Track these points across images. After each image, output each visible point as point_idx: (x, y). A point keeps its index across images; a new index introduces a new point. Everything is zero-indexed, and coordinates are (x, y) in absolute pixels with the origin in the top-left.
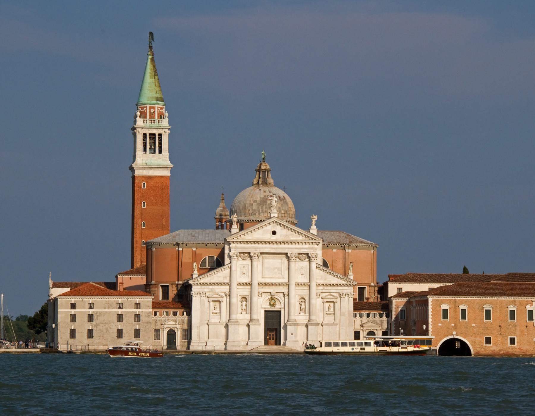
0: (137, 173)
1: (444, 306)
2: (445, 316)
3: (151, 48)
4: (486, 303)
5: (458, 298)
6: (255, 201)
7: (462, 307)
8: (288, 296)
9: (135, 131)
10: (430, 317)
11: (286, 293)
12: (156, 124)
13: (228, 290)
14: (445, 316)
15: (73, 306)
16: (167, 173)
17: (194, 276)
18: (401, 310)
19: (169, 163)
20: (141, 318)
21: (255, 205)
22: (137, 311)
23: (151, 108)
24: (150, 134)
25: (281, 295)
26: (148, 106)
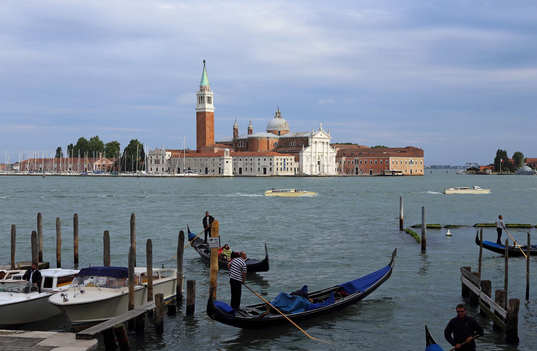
0: (207, 110)
1: (393, 160)
3: (204, 65)
4: (402, 159)
5: (396, 158)
6: (284, 123)
9: (205, 95)
12: (210, 93)
13: (310, 154)
14: (393, 164)
15: (277, 160)
16: (213, 111)
17: (304, 149)
19: (213, 107)
23: (208, 87)
25: (321, 156)
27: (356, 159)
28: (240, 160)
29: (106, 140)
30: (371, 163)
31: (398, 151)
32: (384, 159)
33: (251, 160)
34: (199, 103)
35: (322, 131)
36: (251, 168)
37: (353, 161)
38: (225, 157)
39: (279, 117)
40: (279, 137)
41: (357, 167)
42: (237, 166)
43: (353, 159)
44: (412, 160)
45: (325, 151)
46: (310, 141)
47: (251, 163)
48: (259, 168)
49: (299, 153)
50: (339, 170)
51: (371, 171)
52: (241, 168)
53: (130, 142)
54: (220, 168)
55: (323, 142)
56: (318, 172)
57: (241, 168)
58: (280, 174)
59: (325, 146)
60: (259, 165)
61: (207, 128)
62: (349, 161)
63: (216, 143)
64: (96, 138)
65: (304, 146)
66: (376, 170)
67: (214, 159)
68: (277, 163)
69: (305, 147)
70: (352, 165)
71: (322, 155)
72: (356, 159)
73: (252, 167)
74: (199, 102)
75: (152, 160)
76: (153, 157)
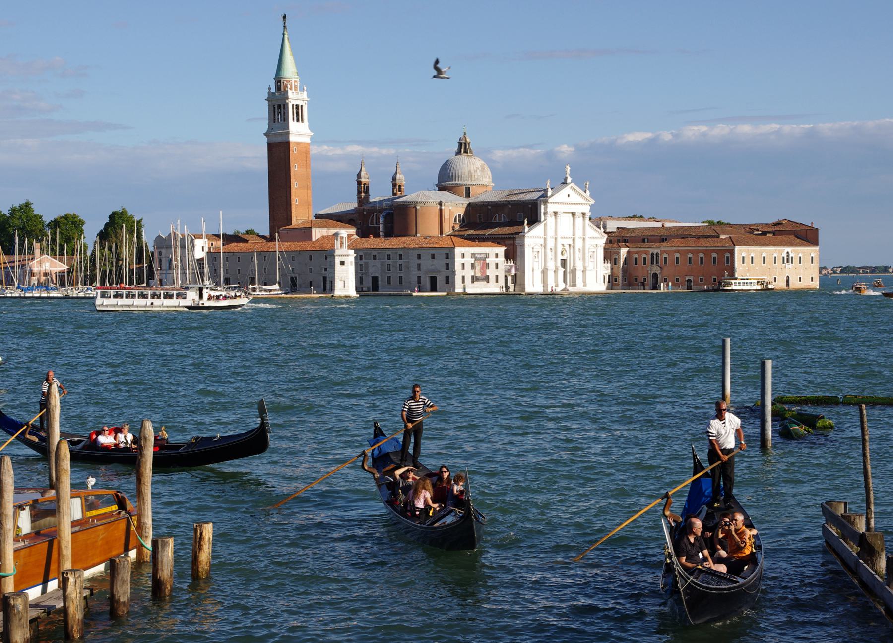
0: (292, 138)
1: (743, 255)
2: (743, 263)
3: (285, 27)
6: (478, 168)
7: (752, 255)
8: (574, 247)
10: (736, 262)
11: (572, 245)
12: (300, 97)
13: (542, 243)
14: (743, 263)
15: (463, 256)
18: (625, 258)
19: (308, 131)
20: (499, 266)
21: (478, 171)
22: (497, 260)
24: (296, 105)
26: (293, 80)
27: (653, 254)
28: (375, 259)
29: (47, 211)
30: (690, 263)
31: (756, 233)
32: (720, 252)
33: (401, 257)
34: (275, 122)
35: (570, 186)
36: (401, 278)
37: (645, 258)
38: (337, 252)
39: (467, 153)
40: (468, 202)
41: (654, 272)
42: (366, 273)
43: (646, 253)
44: (790, 253)
45: (579, 233)
46: (543, 210)
47: (401, 265)
48: (419, 277)
49: (514, 239)
50: (612, 280)
51: (689, 281)
52: (377, 278)
53: (110, 217)
54: (325, 278)
55: (572, 213)
56: (561, 286)
57: (377, 278)
58: (469, 291)
59: (579, 221)
60: (419, 269)
61: (292, 180)
62: (636, 259)
63: (317, 217)
64: (26, 207)
65: (526, 222)
66: (701, 280)
67: (310, 256)
68: (463, 264)
69: (530, 224)
70: (643, 267)
71: (571, 242)
72: (653, 254)
73: (402, 275)
74: (272, 117)
75: (163, 260)
76: (164, 251)
